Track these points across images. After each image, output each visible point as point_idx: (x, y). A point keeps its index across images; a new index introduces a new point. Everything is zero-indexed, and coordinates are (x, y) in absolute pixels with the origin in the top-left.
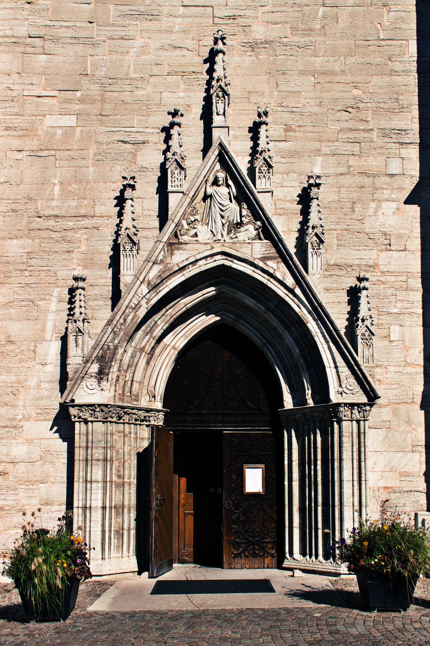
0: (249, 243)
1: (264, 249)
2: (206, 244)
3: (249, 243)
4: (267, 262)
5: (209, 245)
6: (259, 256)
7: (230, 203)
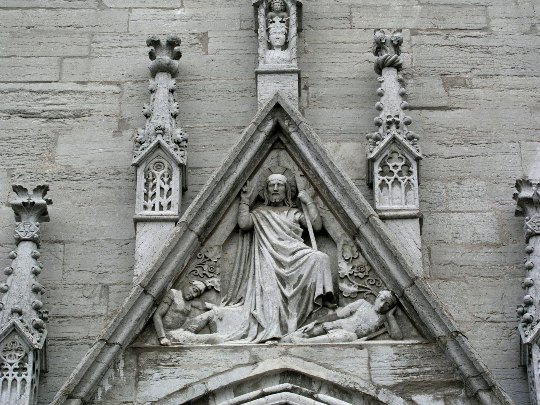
0: (361, 347)
1: (405, 363)
2: (235, 349)
3: (361, 347)
4: (415, 398)
5: (247, 354)
6: (389, 382)
7: (304, 246)
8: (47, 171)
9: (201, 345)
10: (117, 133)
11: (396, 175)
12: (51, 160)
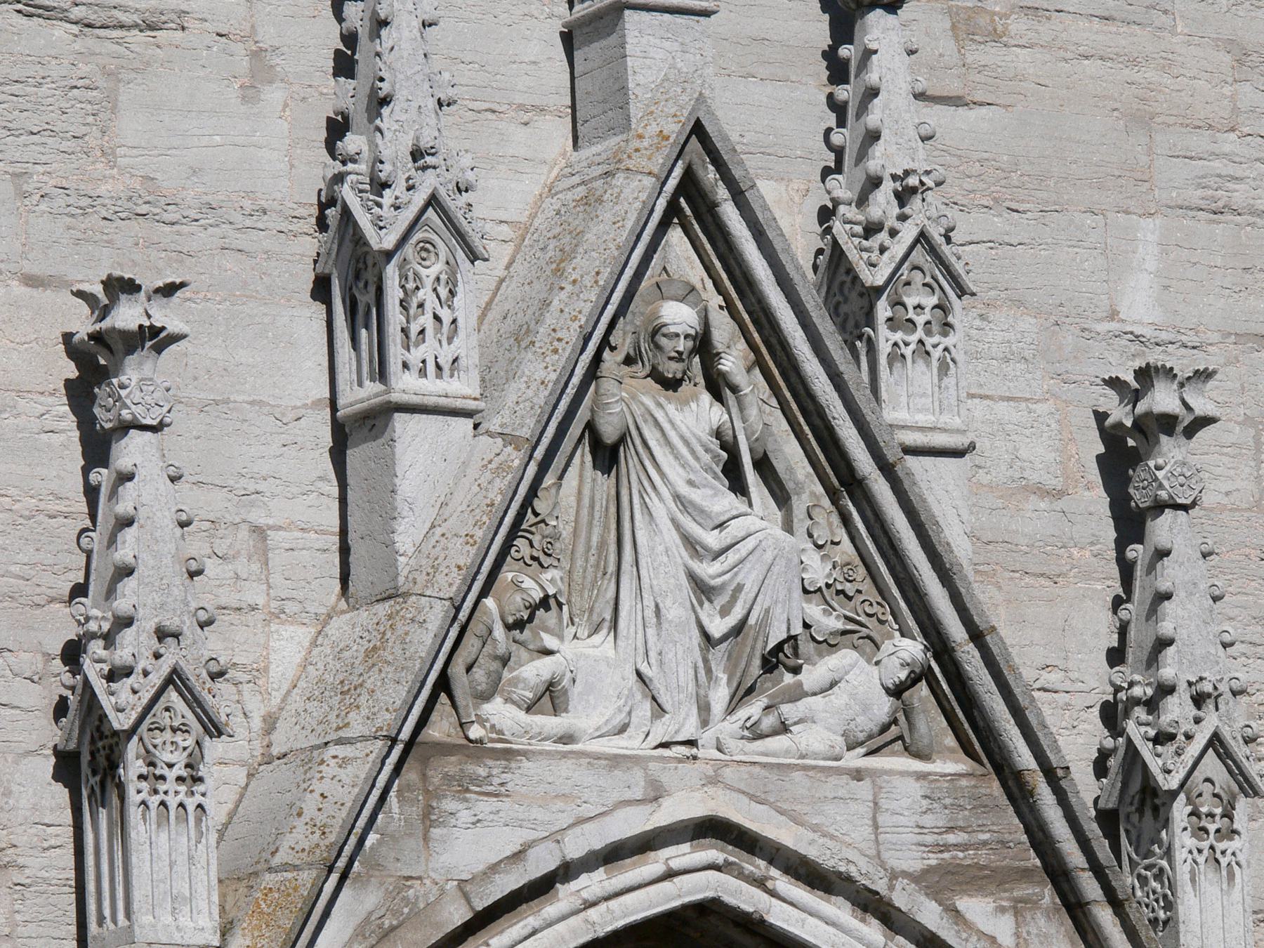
0: (858, 775)
2: (616, 761)
5: (638, 776)
6: (913, 861)
8: (103, 189)
9: (549, 746)
10: (250, 93)
11: (920, 333)
12: (108, 155)
